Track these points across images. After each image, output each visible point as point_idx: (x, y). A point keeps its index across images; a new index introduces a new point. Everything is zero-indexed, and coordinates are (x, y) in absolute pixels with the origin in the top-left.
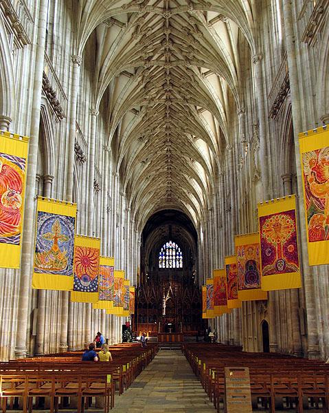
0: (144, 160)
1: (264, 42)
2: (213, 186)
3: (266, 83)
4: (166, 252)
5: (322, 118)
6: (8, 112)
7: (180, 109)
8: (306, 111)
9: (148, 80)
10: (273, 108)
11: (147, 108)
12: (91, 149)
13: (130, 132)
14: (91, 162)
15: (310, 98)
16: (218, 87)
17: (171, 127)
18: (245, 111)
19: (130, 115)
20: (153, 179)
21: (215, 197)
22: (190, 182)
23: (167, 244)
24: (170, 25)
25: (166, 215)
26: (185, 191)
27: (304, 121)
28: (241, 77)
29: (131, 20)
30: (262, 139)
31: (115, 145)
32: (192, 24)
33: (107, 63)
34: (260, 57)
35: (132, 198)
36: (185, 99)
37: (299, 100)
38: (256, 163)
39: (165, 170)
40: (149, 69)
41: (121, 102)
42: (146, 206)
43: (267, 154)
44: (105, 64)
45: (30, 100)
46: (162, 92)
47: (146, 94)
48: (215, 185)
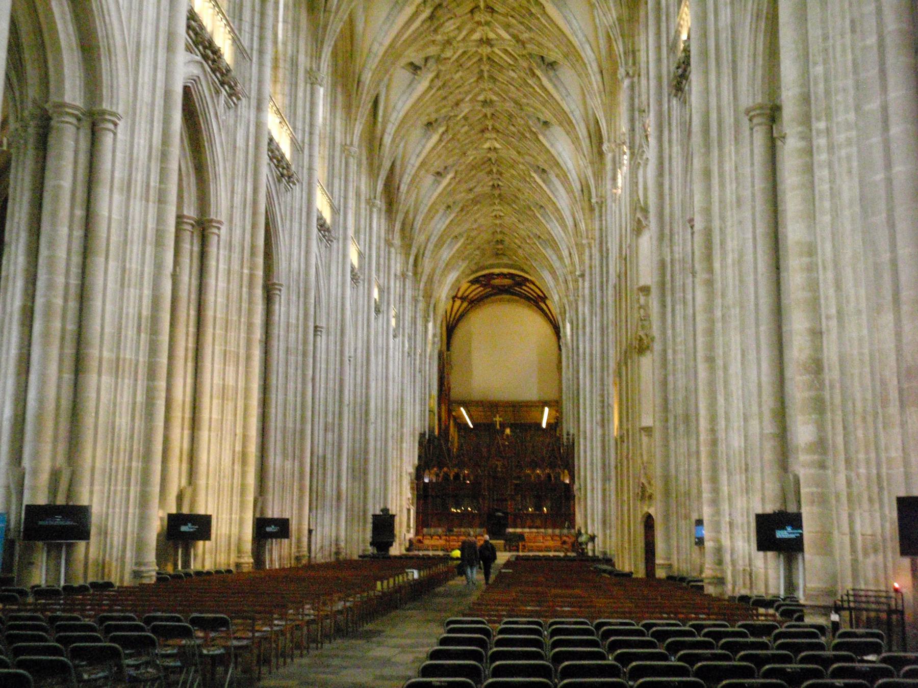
3: (667, 19)
5: (747, 112)
6: (115, 101)
7: (512, 63)
8: (719, 95)
10: (675, 77)
13: (401, 115)
15: (726, 70)
17: (494, 98)
19: (401, 76)
20: (462, 210)
21: (587, 251)
27: (714, 116)
30: (652, 141)
31: (373, 142)
36: (518, 41)
37: (706, 73)
39: (487, 189)
41: (379, 50)
42: (448, 267)
43: (660, 173)
45: (161, 75)
46: (469, 26)
47: (435, 31)
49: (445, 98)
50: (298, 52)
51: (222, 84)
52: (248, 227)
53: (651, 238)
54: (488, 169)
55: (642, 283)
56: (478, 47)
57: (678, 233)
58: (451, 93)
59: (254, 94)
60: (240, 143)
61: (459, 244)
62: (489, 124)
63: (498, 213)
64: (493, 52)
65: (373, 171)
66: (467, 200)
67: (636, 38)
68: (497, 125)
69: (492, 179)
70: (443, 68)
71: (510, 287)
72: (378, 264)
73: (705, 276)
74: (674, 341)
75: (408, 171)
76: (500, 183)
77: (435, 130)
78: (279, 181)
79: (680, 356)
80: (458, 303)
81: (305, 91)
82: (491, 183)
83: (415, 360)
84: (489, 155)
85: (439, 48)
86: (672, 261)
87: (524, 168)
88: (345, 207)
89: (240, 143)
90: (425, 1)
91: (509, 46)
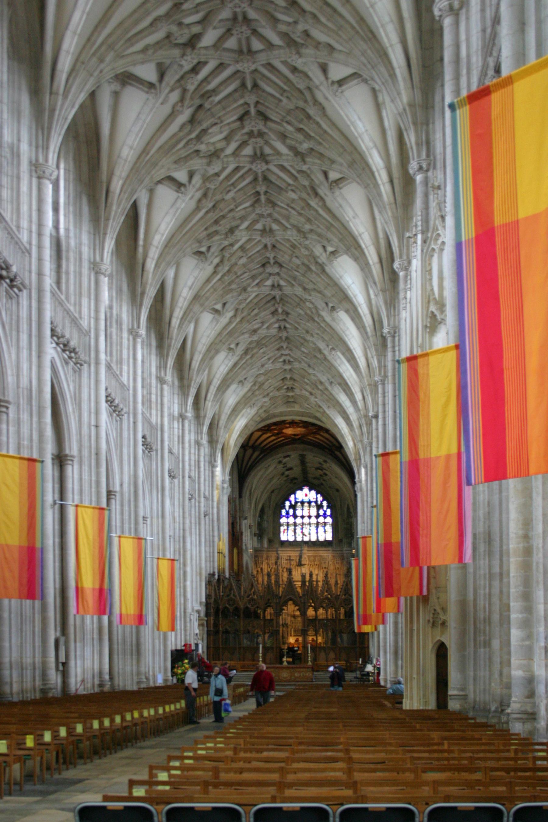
0: (219, 307)
7: (290, 181)
9: (197, 102)
11: (206, 179)
16: (374, 117)
17: (275, 227)
20: (246, 352)
22: (329, 358)
23: (299, 493)
26: (324, 379)
39: (273, 331)
40: (195, 70)
47: (199, 138)
49: (216, 222)
54: (273, 309)
56: (252, 163)
58: (223, 217)
61: (246, 390)
62: (271, 255)
63: (287, 358)
64: (268, 170)
66: (251, 343)
67: (431, 126)
68: (281, 259)
69: (278, 320)
71: (304, 436)
76: (287, 326)
80: (249, 451)
82: (276, 325)
84: (273, 293)
87: (311, 306)
91: (287, 160)
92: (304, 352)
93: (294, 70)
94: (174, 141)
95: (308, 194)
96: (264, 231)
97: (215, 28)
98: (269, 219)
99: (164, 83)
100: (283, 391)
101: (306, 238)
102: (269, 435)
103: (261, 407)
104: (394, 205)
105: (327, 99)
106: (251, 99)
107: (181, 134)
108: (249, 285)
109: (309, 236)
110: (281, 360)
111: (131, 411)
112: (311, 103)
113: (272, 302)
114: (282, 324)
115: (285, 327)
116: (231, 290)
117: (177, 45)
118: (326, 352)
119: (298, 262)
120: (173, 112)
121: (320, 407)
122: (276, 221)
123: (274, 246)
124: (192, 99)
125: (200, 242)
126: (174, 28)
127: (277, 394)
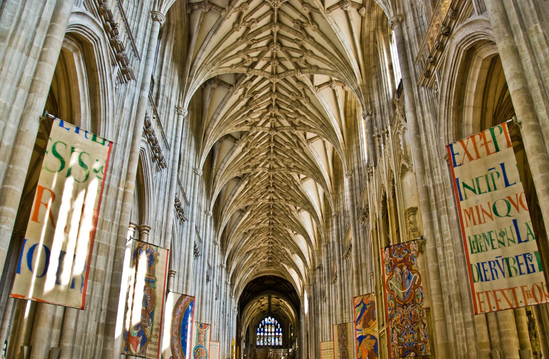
1: (403, 4)
2: (323, 236)
4: (264, 329)
7: (287, 140)
9: (250, 96)
12: (174, 154)
14: (173, 170)
17: (276, 166)
18: (370, 115)
20: (253, 236)
22: (294, 238)
23: (266, 320)
24: (279, 21)
25: (266, 282)
26: (288, 251)
28: (366, 75)
29: (232, 4)
30: (409, 115)
32: (306, 12)
33: (203, 56)
34: (400, 19)
35: (228, 253)
36: (293, 125)
38: (402, 148)
39: (267, 225)
40: (252, 80)
43: (418, 132)
44: (199, 56)
47: (248, 114)
48: (325, 235)
49: (250, 161)
50: (171, 96)
51: (118, 59)
52: (126, 159)
53: (415, 174)
54: (268, 212)
55: (408, 207)
56: (270, 131)
57: (437, 167)
58: (253, 158)
59: (140, 80)
60: (127, 105)
65: (209, 195)
70: (251, 141)
72: (209, 254)
73: (532, 123)
74: (442, 241)
75: (227, 204)
76: (274, 222)
77: (243, 181)
78: (153, 161)
79: (450, 251)
80: (246, 294)
81: (174, 116)
82: (268, 222)
83: (225, 316)
85: (249, 127)
86: (434, 187)
88: (193, 203)
89: (127, 105)
90: (264, 2)
91: (287, 129)
92: (280, 236)
93: (297, 81)
94: (238, 114)
95: (296, 146)
96: (270, 169)
97: (263, 60)
98: (273, 162)
99: (237, 84)
100: (266, 260)
101: (291, 171)
102: (256, 284)
103: (255, 268)
104: (344, 144)
105: (312, 93)
106: (275, 97)
107: (241, 111)
108: (259, 198)
109: (293, 170)
110: (268, 241)
111: (203, 254)
112: (304, 97)
113: (268, 209)
114: (271, 221)
115: (272, 223)
116: (251, 199)
117: (245, 67)
118: (292, 235)
119: (285, 184)
120: (239, 99)
121: (284, 268)
122: (277, 163)
123: (273, 177)
124: (248, 94)
125: (240, 171)
126: (246, 57)
127: (263, 260)
